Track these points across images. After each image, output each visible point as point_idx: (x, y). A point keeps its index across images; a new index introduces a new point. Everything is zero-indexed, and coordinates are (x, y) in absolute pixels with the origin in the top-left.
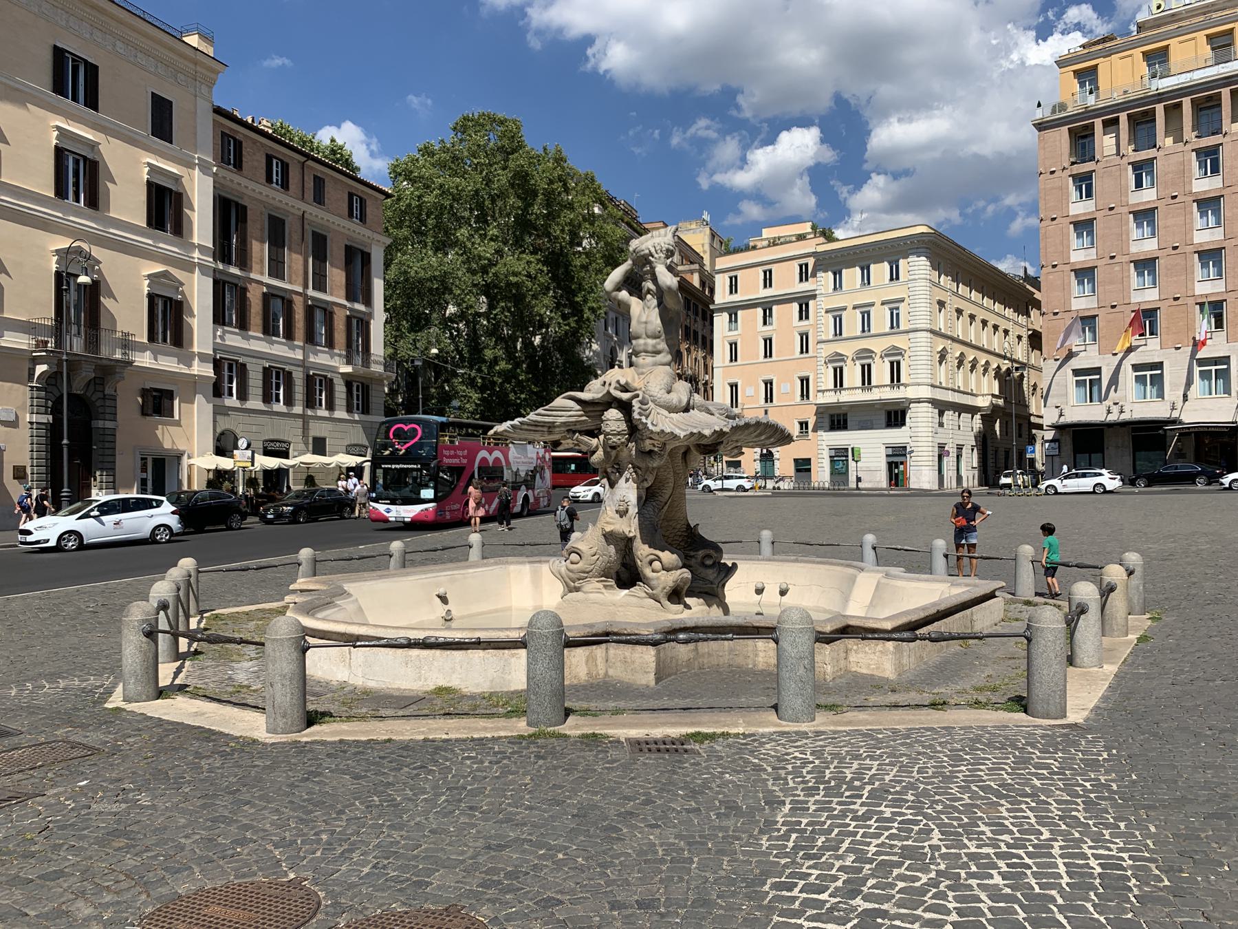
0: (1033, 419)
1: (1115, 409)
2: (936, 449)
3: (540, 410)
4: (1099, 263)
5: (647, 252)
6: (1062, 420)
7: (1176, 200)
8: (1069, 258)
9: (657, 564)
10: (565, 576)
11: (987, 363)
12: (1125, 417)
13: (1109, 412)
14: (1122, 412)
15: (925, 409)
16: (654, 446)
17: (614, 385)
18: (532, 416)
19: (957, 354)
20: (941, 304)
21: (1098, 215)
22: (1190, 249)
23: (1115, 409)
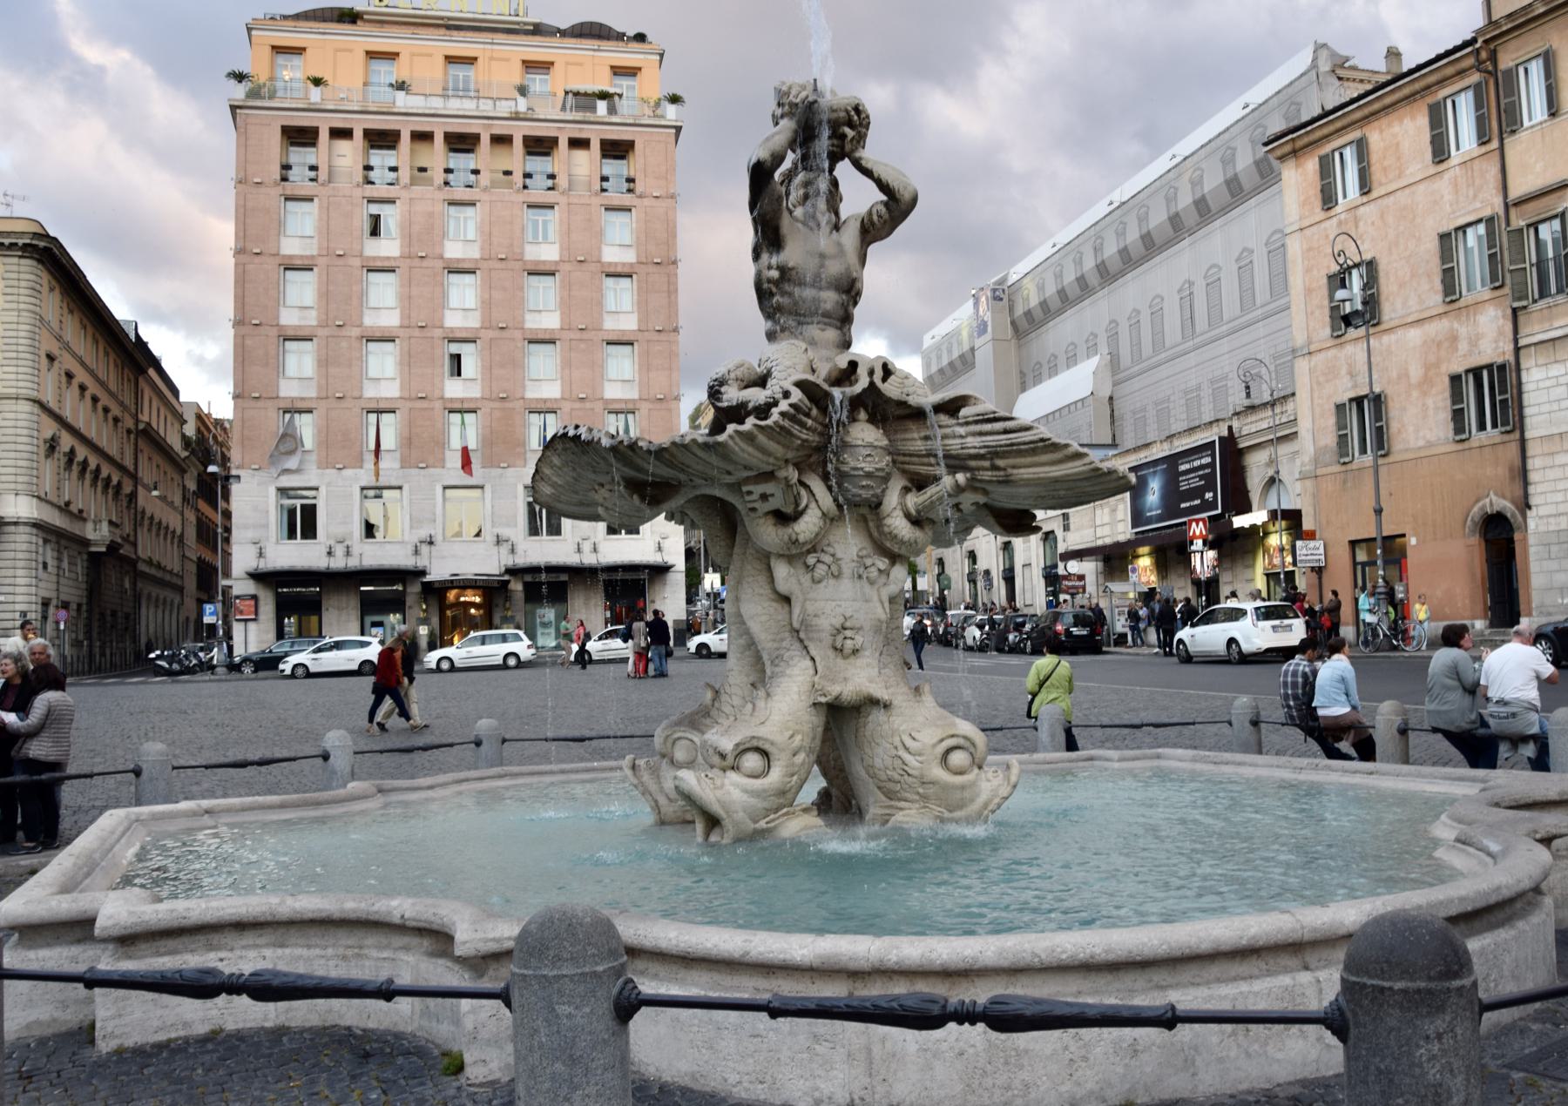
0: (142, 567)
1: (339, 551)
2: (39, 607)
4: (321, 332)
5: (842, 114)
7: (425, 263)
8: (277, 317)
9: (958, 758)
11: (98, 470)
12: (353, 563)
13: (329, 553)
14: (348, 553)
15: (24, 538)
19: (67, 449)
20: (51, 358)
21: (322, 261)
22: (438, 333)
23: (339, 551)
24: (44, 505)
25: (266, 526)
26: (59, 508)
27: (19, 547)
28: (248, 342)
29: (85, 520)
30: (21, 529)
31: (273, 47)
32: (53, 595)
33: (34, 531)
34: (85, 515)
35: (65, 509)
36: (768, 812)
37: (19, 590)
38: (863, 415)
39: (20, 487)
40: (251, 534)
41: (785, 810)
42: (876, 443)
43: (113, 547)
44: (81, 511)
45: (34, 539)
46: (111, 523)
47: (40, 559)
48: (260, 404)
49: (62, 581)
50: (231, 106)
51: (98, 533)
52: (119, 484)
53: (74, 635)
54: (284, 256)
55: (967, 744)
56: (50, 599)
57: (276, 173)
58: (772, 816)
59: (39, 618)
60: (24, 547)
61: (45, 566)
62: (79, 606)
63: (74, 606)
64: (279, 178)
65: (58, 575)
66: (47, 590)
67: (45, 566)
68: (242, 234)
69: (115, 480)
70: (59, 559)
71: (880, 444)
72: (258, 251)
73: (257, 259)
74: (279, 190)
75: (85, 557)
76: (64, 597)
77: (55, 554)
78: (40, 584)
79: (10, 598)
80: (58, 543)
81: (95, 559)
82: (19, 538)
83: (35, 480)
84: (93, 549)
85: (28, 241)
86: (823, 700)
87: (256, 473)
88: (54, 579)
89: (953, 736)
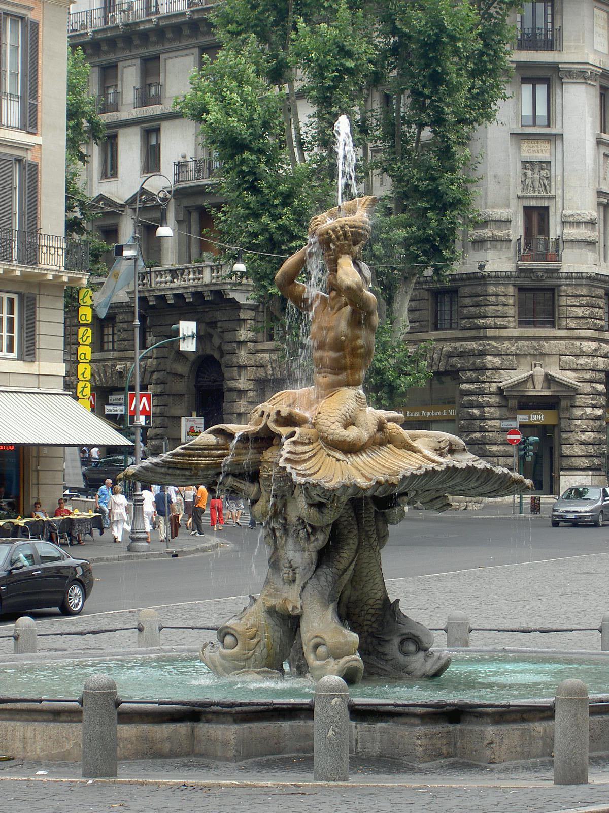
9: (321, 650)
10: (217, 664)
89: (316, 637)
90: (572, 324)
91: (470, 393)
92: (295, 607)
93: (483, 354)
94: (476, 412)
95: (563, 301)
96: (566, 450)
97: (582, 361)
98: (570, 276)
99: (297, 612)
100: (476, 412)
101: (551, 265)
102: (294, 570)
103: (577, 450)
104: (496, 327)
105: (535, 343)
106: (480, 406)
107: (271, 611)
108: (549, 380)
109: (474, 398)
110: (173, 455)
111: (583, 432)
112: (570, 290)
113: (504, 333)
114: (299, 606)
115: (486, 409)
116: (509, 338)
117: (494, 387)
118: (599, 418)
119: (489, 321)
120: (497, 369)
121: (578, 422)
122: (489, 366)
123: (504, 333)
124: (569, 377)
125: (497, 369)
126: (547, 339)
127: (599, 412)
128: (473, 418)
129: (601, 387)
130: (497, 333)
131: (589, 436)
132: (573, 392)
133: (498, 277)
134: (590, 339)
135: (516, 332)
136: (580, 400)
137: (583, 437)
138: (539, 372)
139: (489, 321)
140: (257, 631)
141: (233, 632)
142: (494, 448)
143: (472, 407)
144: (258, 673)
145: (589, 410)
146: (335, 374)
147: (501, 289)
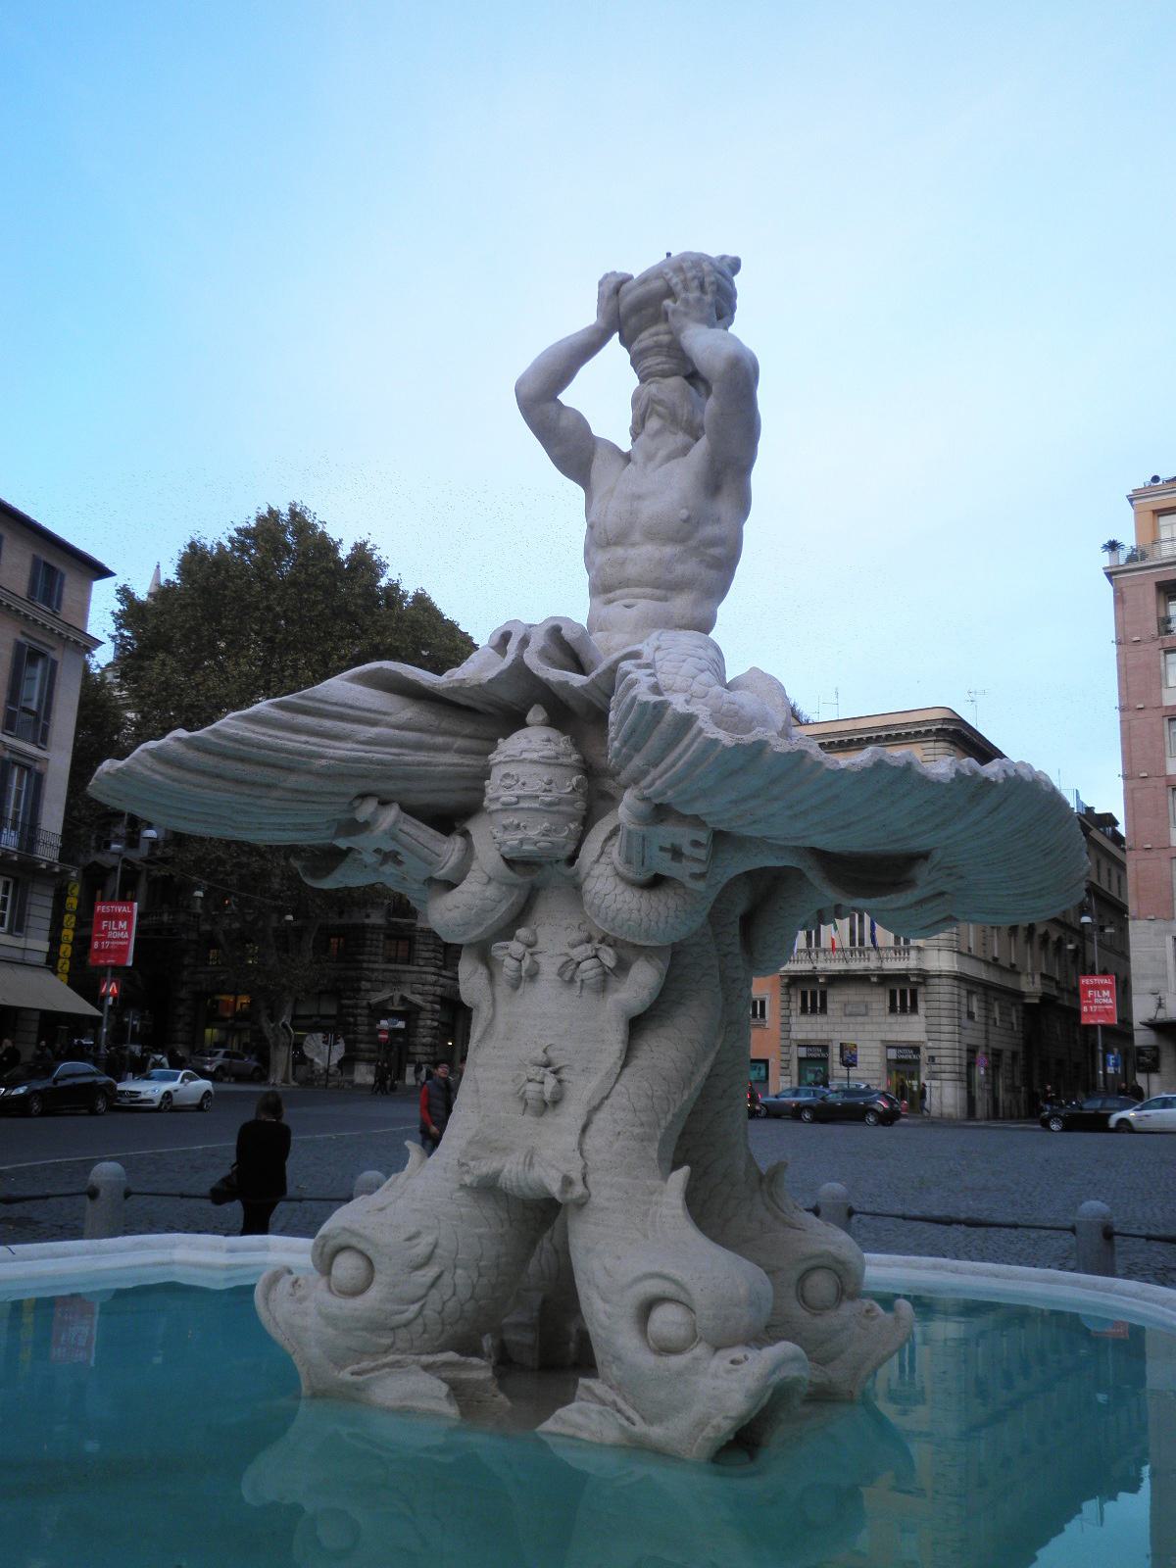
2: (964, 1054)
3: (263, 706)
5: (658, 284)
6: (1161, 1016)
8: (1164, 768)
9: (667, 1320)
15: (947, 989)
16: (676, 853)
17: (538, 642)
18: (229, 723)
24: (966, 958)
25: (1165, 976)
26: (986, 963)
27: (943, 997)
28: (1138, 795)
29: (1019, 974)
30: (944, 981)
31: (1154, 512)
32: (982, 1042)
33: (956, 983)
34: (1018, 969)
35: (993, 964)
36: (361, 1353)
37: (944, 1037)
38: (536, 714)
39: (941, 943)
40: (1149, 985)
41: (391, 1358)
42: (525, 755)
43: (1047, 1000)
44: (1013, 966)
45: (956, 991)
46: (1043, 976)
47: (964, 1009)
48: (1153, 854)
49: (991, 1029)
50: (1106, 574)
51: (1031, 986)
52: (1060, 939)
53: (1009, 1082)
54: (1167, 707)
55: (683, 1297)
56: (977, 1047)
57: (1153, 626)
58: (364, 1365)
59: (965, 1063)
60: (947, 997)
61: (971, 1015)
62: (1014, 1055)
63: (1008, 1054)
64: (1155, 632)
65: (986, 1024)
66: (974, 1036)
67: (971, 1015)
68: (1124, 693)
69: (1054, 936)
70: (988, 1009)
71: (535, 756)
72: (1141, 706)
73: (1141, 714)
74: (1158, 645)
75: (1020, 1008)
76: (993, 1044)
77: (983, 1005)
78: (964, 1032)
79: (936, 1044)
80: (985, 994)
81: (1029, 1009)
82: (942, 989)
83: (955, 937)
84: (1027, 1001)
85: (939, 727)
86: (468, 1179)
87: (1151, 923)
88: (983, 1027)
90: (421, 963)
91: (349, 1007)
92: (567, 1182)
93: (359, 980)
94: (351, 1020)
95: (417, 946)
96: (412, 1049)
97: (427, 988)
98: (422, 930)
99: (578, 1190)
100: (351, 1020)
101: (413, 921)
102: (555, 1072)
103: (419, 1049)
104: (369, 962)
105: (395, 974)
106: (354, 1016)
107: (488, 1189)
108: (403, 999)
109: (351, 1010)
110: (249, 719)
111: (424, 1037)
112: (422, 940)
113: (376, 966)
114: (576, 1175)
115: (359, 1018)
116: (377, 970)
117: (365, 1003)
118: (435, 1028)
119: (366, 958)
120: (368, 991)
121: (422, 1030)
122: (363, 988)
123: (376, 966)
124: (417, 999)
125: (368, 991)
126: (404, 972)
127: (436, 1024)
128: (350, 1024)
129: (437, 1007)
130: (371, 966)
131: (428, 1040)
132: (418, 1009)
133: (374, 927)
134: (433, 974)
135: (383, 966)
136: (423, 1015)
137: (424, 1040)
138: (397, 995)
139: (366, 958)
140: (436, 1246)
141: (362, 1246)
142: (362, 1046)
143: (349, 1016)
144: (427, 1368)
145: (429, 1022)
146: (659, 599)
147: (375, 936)
